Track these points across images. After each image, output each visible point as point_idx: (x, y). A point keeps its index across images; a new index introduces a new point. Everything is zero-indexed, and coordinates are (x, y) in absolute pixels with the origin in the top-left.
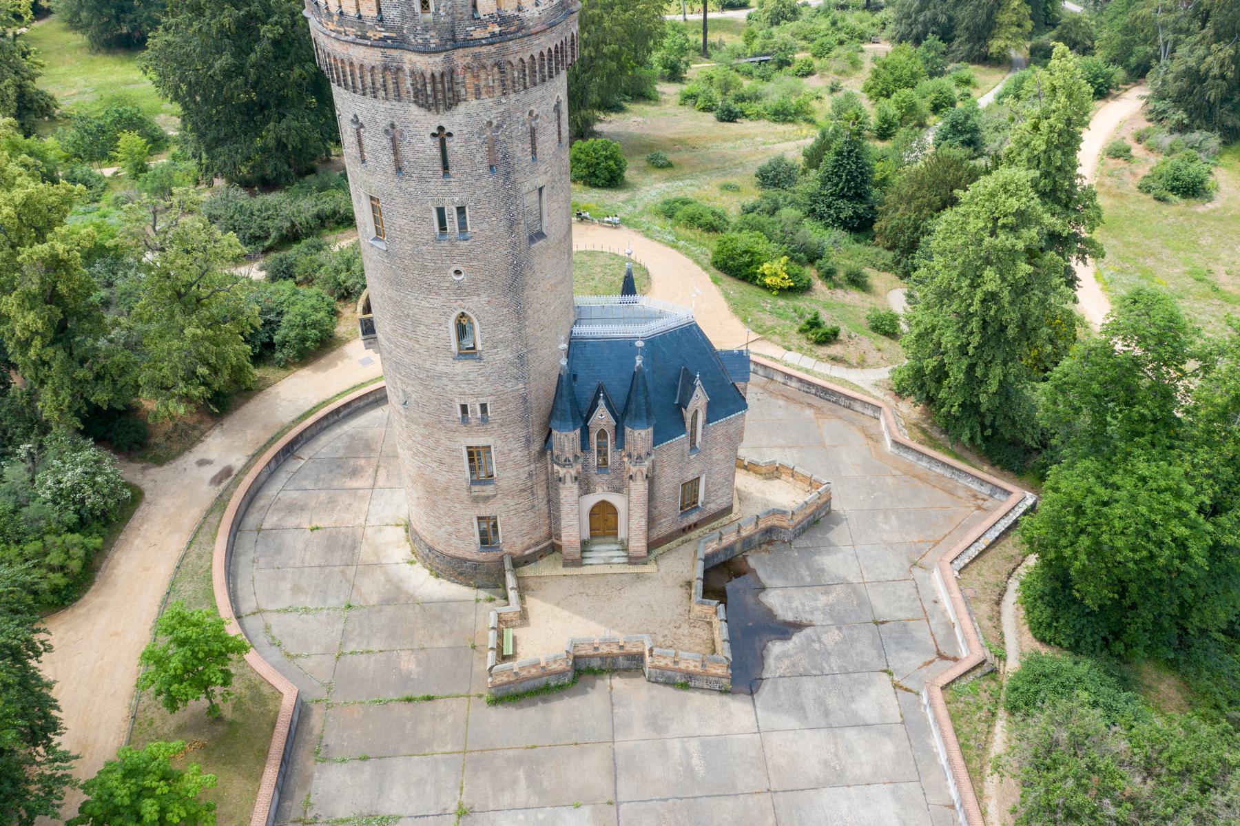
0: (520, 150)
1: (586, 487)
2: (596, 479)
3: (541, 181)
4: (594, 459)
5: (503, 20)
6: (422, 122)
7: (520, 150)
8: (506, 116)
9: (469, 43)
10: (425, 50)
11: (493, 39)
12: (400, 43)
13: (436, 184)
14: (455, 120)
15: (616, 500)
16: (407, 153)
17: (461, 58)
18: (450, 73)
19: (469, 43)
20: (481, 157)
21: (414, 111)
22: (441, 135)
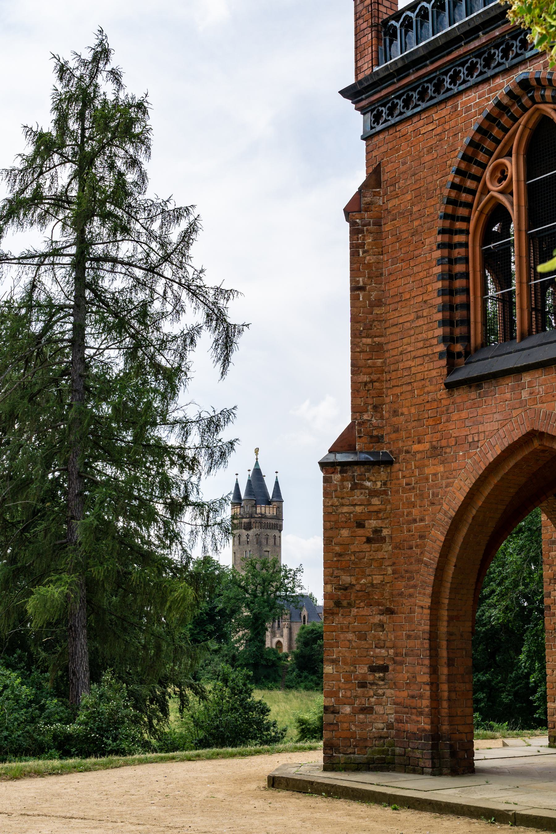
0: (264, 541)
1: (274, 635)
2: (277, 632)
3: (268, 550)
4: (276, 625)
5: (261, 514)
6: (245, 533)
7: (264, 541)
8: (261, 533)
9: (255, 517)
10: (246, 518)
11: (259, 517)
12: (243, 518)
13: (246, 546)
14: (251, 532)
15: (281, 640)
16: (241, 540)
17: (253, 520)
18: (250, 523)
19: (255, 517)
20: (255, 540)
21: (244, 531)
22: (248, 536)
